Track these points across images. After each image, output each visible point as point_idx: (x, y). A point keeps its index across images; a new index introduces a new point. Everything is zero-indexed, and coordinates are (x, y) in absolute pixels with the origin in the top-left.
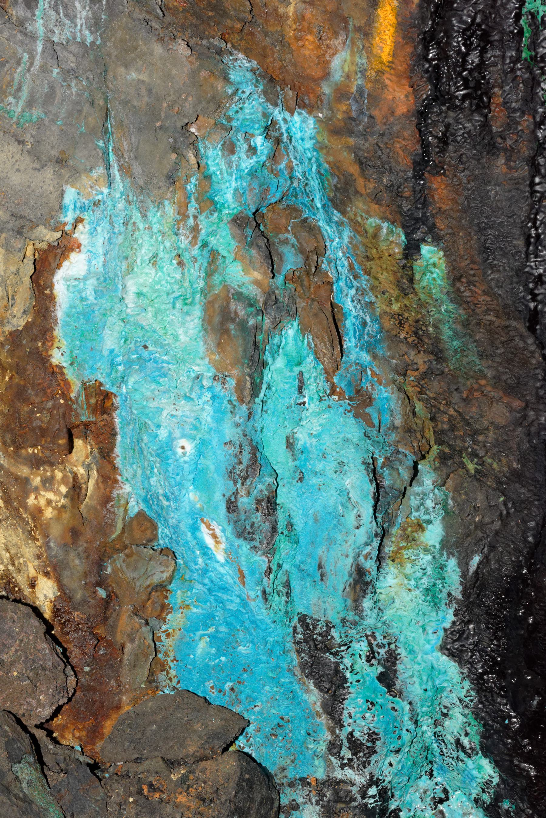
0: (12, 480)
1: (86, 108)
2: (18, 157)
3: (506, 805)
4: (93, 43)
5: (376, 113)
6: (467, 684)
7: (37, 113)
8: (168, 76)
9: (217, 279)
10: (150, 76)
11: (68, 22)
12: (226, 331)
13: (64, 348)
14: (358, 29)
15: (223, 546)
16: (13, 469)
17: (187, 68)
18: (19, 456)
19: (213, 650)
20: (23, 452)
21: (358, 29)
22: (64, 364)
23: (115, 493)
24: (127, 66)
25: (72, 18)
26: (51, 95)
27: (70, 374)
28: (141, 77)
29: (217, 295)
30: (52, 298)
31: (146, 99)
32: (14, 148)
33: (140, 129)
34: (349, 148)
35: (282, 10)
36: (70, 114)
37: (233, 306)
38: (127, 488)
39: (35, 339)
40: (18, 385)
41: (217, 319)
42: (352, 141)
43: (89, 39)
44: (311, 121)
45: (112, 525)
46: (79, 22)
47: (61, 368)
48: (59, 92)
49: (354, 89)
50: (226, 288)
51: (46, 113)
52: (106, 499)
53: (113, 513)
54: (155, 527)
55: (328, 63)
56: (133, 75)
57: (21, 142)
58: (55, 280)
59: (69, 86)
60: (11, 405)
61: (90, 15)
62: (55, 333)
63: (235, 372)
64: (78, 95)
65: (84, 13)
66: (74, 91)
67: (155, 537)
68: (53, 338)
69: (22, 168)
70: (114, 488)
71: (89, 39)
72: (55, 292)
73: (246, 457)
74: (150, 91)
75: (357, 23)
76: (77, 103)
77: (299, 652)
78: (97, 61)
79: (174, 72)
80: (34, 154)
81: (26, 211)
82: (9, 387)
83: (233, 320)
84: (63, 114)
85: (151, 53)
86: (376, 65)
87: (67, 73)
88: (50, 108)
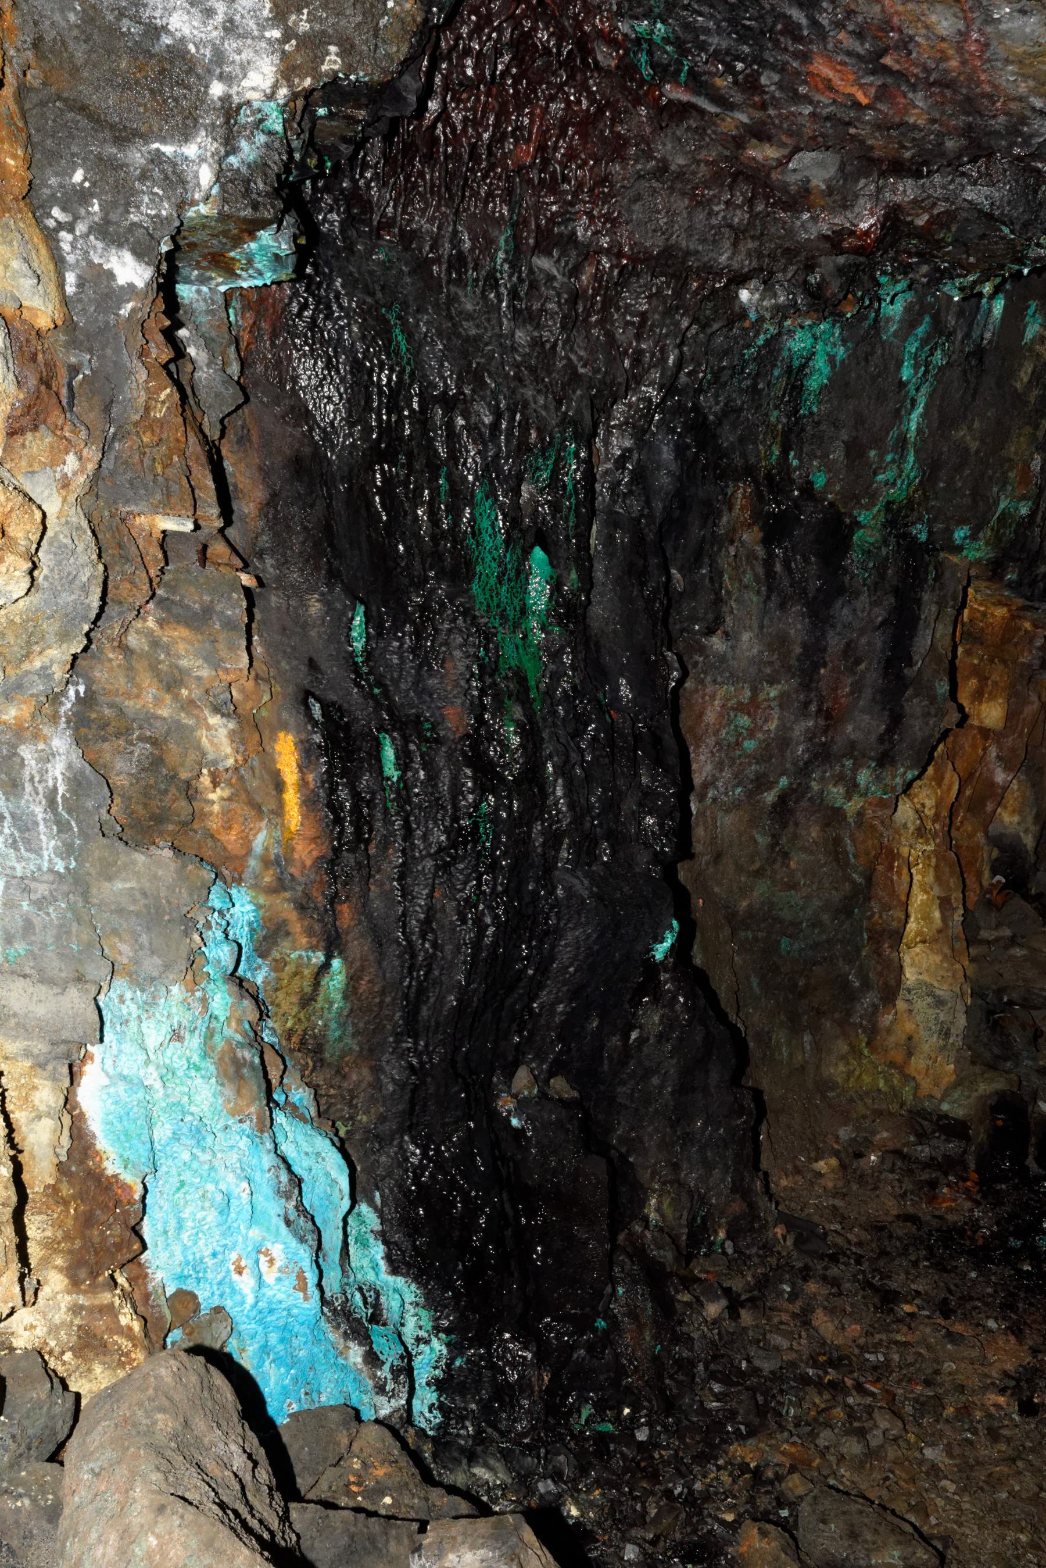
0: (97, 1316)
1: (75, 927)
2: (31, 990)
3: (458, 1363)
4: (67, 868)
5: (293, 870)
6: (413, 1287)
7: (20, 947)
8: (155, 877)
9: (217, 1038)
10: (139, 882)
11: (33, 856)
12: (241, 1077)
13: (113, 1156)
14: (272, 812)
15: (278, 1264)
16: (97, 1302)
17: (173, 866)
18: (96, 1287)
19: (282, 1370)
20: (101, 1279)
21: (272, 812)
22: (118, 1171)
23: (150, 1288)
24: (110, 879)
25: (38, 852)
26: (28, 927)
27: (128, 1177)
28: (128, 885)
29: (223, 1051)
30: (82, 1115)
31: (143, 901)
32: (21, 983)
33: (149, 929)
34: (288, 900)
35: (207, 809)
36: (58, 938)
37: (239, 1055)
38: (159, 1275)
39: (82, 1162)
40: (84, 1212)
41: (231, 1070)
42: (287, 895)
43: (60, 867)
44: (243, 890)
45: (162, 1317)
46: (45, 853)
47: (116, 1176)
48: (36, 921)
49: (273, 857)
50: (229, 1041)
51: (30, 944)
52: (147, 1296)
53: (158, 1306)
54: (194, 1297)
55: (250, 842)
56: (119, 885)
57: (25, 976)
58: (79, 1099)
59: (48, 914)
60: (83, 1237)
61: (59, 844)
62: (98, 1147)
63: (253, 1109)
64: (58, 918)
65: (53, 843)
66: (53, 916)
67: (199, 1305)
68: (97, 1153)
69: (43, 998)
70: (145, 1285)
71: (60, 867)
72: (85, 1108)
73: (284, 1177)
74: (145, 894)
75: (270, 807)
76: (61, 926)
77: (337, 1327)
78: (77, 881)
79: (160, 873)
80: (45, 980)
81: (65, 1035)
82: (76, 1218)
83: (244, 1065)
84: (50, 940)
85: (134, 863)
86: (287, 835)
87: (40, 904)
88: (33, 938)
